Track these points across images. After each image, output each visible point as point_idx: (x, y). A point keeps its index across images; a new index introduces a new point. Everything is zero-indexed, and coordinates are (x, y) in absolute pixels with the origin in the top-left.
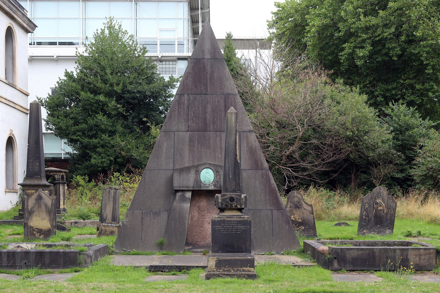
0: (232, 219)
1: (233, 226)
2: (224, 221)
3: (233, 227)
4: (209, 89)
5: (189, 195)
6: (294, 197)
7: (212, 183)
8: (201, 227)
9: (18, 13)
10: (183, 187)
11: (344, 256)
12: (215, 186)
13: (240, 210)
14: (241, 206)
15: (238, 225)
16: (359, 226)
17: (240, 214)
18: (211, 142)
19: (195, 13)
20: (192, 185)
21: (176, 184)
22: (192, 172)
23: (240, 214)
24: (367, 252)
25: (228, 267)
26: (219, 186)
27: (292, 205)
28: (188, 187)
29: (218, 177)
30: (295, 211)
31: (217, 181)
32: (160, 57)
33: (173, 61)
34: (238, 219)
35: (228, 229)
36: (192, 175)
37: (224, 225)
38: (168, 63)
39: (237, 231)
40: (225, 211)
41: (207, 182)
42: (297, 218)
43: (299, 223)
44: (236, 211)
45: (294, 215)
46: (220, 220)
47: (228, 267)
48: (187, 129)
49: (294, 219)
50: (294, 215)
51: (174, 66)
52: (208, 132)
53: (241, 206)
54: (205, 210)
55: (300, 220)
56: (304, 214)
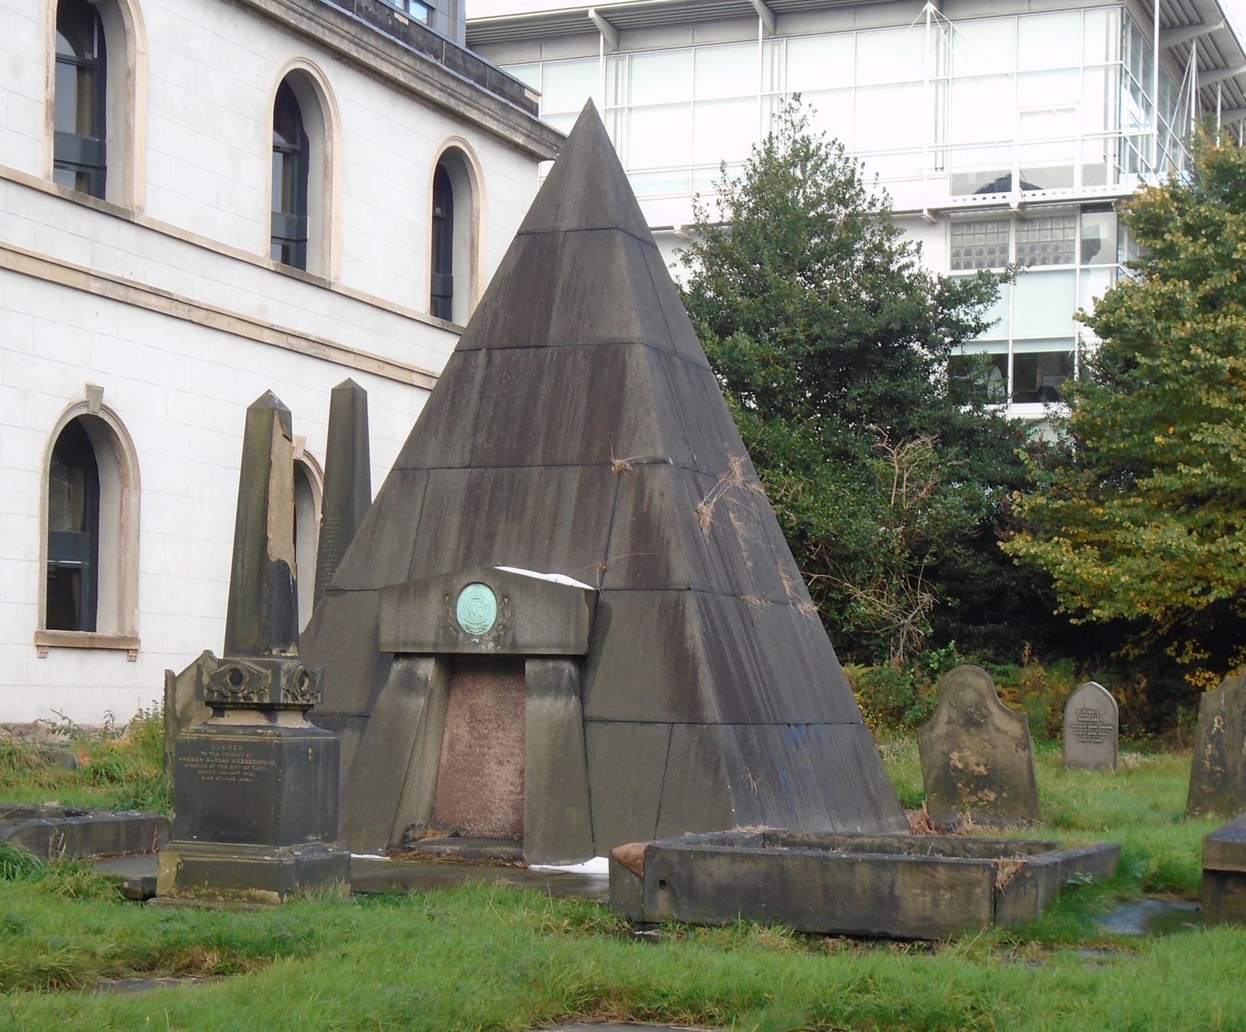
1: (230, 759)
3: (230, 763)
4: (553, 330)
5: (427, 669)
6: (963, 686)
8: (477, 774)
10: (405, 644)
11: (691, 878)
12: (497, 640)
13: (269, 710)
14: (260, 698)
15: (245, 758)
16: (1191, 795)
17: (263, 721)
18: (530, 501)
20: (431, 637)
21: (389, 637)
22: (432, 595)
24: (763, 866)
25: (210, 885)
26: (509, 641)
27: (954, 714)
28: (421, 645)
29: (508, 613)
30: (964, 737)
31: (504, 627)
34: (246, 739)
35: (216, 768)
36: (432, 607)
37: (209, 756)
39: (242, 775)
40: (227, 713)
41: (476, 630)
42: (972, 760)
43: (979, 777)
44: (256, 714)
45: (960, 749)
47: (210, 885)
48: (466, 461)
49: (960, 766)
50: (960, 749)
52: (527, 469)
53: (260, 698)
54: (490, 721)
55: (982, 769)
56: (994, 747)
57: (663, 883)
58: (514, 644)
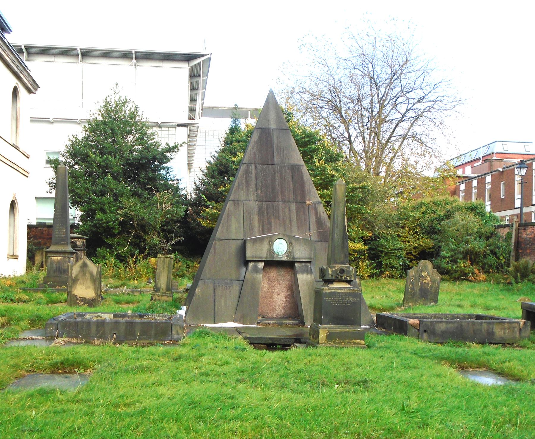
0: (342, 291)
2: (334, 293)
4: (276, 159)
5: (261, 265)
7: (285, 254)
8: (271, 298)
9: (25, 73)
11: (434, 329)
12: (287, 256)
13: (349, 282)
14: (350, 278)
18: (281, 213)
19: (195, 80)
23: (349, 286)
24: (456, 325)
29: (291, 248)
32: (160, 123)
33: (172, 127)
34: (349, 291)
36: (265, 246)
38: (167, 129)
46: (331, 292)
48: (256, 199)
51: (174, 133)
53: (350, 278)
57: (425, 331)
58: (293, 258)
